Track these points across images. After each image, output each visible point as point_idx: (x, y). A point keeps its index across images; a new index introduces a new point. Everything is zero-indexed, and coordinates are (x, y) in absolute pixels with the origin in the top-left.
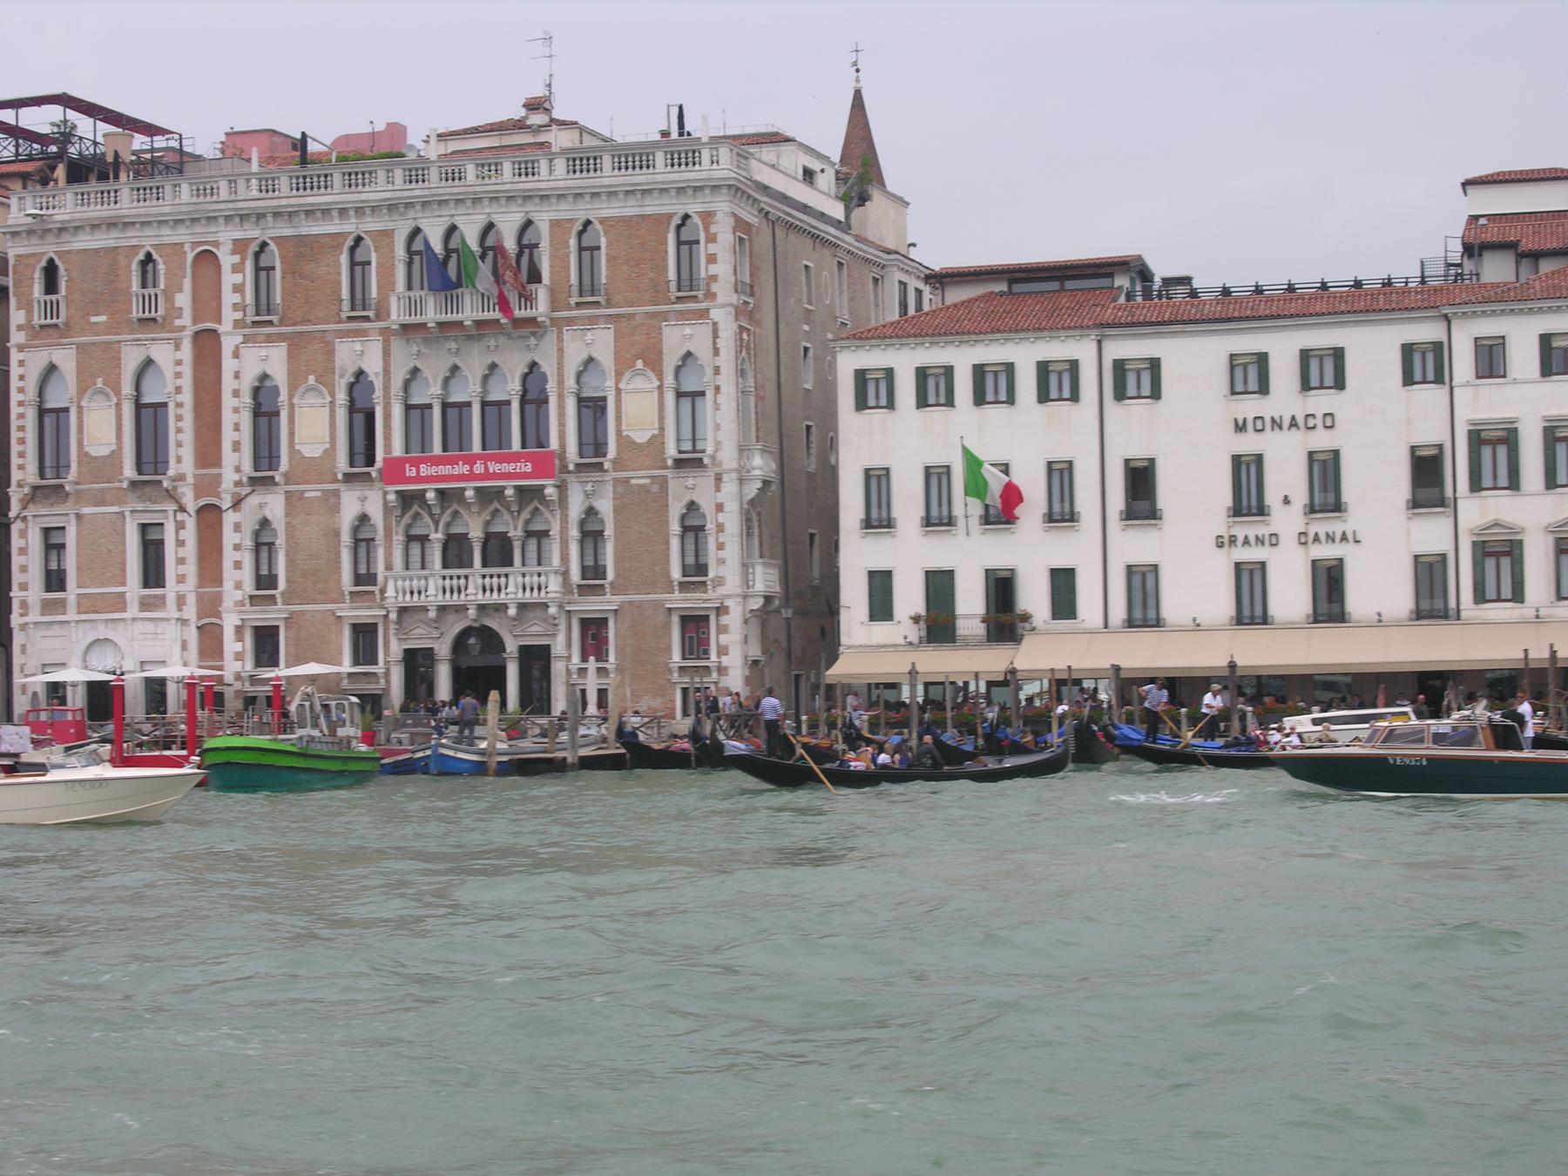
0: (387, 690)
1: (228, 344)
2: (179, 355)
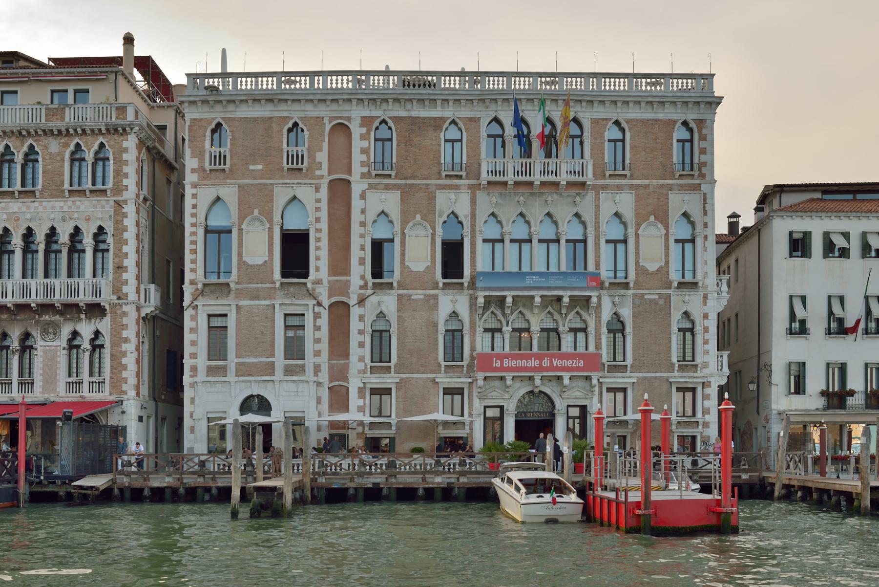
0: (471, 434)
1: (357, 188)
2: (318, 196)
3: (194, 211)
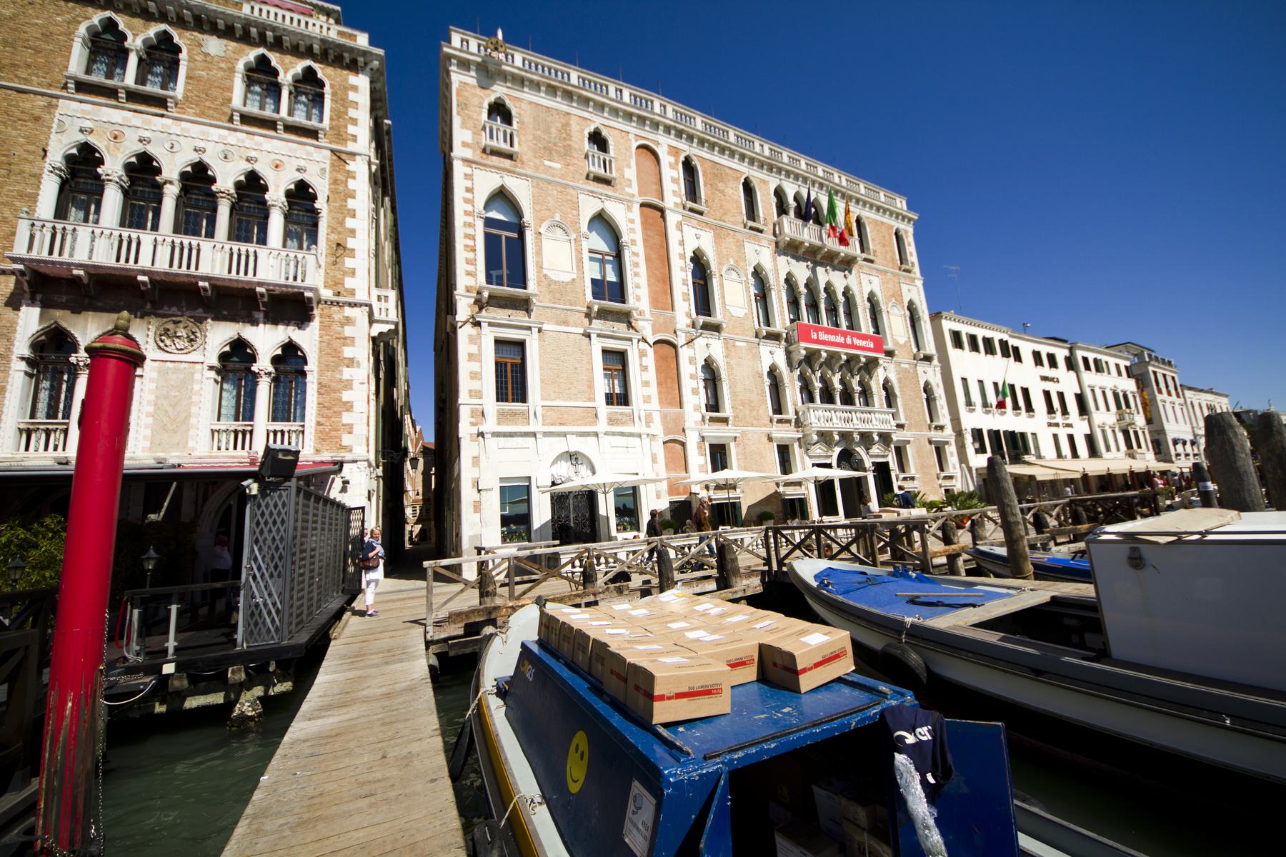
1: (672, 218)
2: (630, 215)
3: (469, 196)
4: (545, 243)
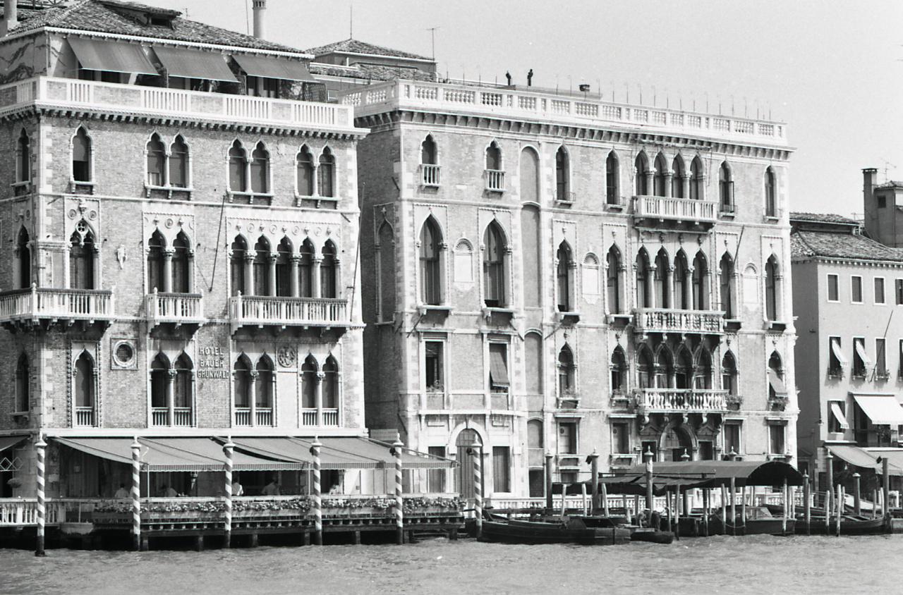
1: (546, 217)
4: (457, 258)
